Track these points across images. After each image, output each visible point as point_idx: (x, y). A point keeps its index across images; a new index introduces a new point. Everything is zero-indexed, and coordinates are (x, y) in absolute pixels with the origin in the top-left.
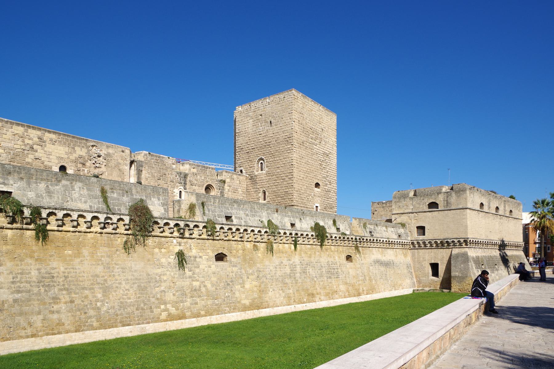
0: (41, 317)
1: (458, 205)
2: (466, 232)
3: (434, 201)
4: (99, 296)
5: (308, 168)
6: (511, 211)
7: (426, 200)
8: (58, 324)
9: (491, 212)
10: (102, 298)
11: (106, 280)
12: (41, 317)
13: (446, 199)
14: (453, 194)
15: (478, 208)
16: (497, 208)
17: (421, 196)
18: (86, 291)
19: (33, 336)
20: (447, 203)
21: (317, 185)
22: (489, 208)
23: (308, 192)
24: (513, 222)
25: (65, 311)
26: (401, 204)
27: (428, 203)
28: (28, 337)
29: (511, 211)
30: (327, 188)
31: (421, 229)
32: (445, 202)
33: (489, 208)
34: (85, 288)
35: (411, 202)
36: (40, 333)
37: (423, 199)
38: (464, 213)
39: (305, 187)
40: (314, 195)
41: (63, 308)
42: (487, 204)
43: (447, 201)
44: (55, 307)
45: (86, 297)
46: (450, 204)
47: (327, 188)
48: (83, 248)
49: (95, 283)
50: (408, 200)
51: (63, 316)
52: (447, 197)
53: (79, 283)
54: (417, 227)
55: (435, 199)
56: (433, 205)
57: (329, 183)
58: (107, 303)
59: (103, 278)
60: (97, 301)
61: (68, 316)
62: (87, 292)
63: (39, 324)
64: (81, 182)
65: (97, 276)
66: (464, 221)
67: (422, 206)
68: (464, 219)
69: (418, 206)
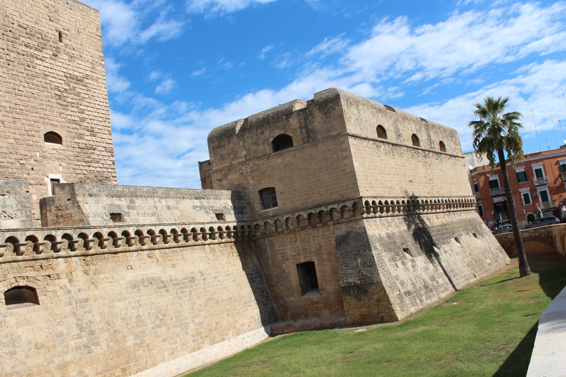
1: (328, 131)
2: (355, 187)
3: (282, 132)
5: (17, 102)
6: (442, 144)
7: (267, 133)
9: (404, 143)
13: (303, 125)
14: (317, 113)
15: (375, 136)
16: (415, 138)
17: (257, 128)
20: (308, 131)
21: (53, 137)
22: (399, 136)
23: (22, 152)
24: (448, 163)
26: (223, 152)
27: (271, 140)
29: (442, 144)
30: (83, 141)
31: (268, 196)
32: (304, 130)
33: (399, 136)
35: (241, 143)
37: (263, 133)
38: (344, 146)
39: (12, 141)
40: (44, 157)
42: (392, 128)
43: (306, 126)
46: (313, 131)
47: (83, 141)
50: (235, 139)
52: (306, 120)
54: (261, 192)
55: (284, 128)
56: (282, 143)
57: (88, 133)
66: (346, 162)
67: (261, 147)
68: (346, 158)
69: (253, 148)
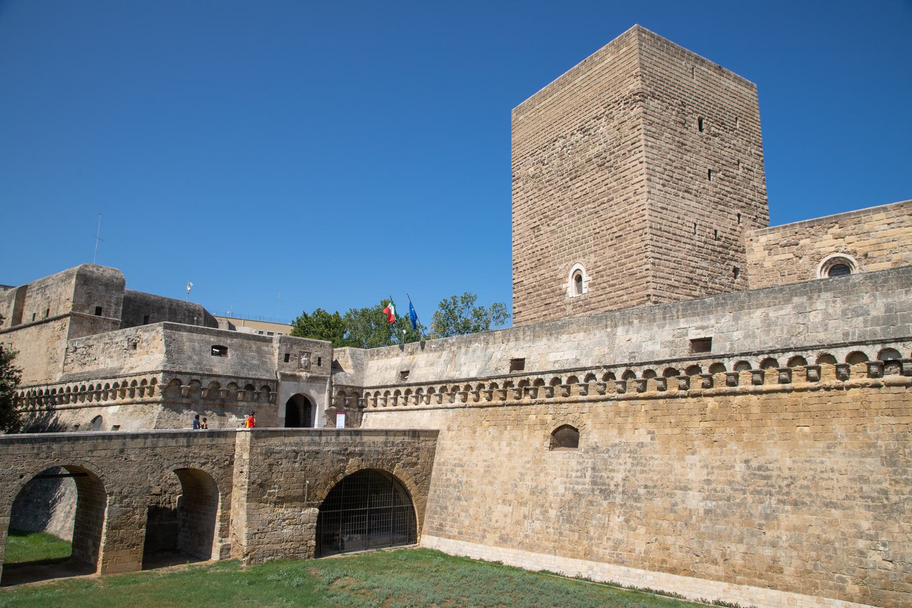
0: (742, 548)
4: (865, 525)
8: (770, 568)
10: (872, 532)
11: (885, 492)
12: (742, 548)
18: (833, 511)
19: (728, 579)
25: (786, 545)
28: (719, 579)
34: (831, 503)
36: (738, 578)
41: (784, 538)
44: (768, 533)
45: (833, 523)
48: (835, 420)
49: (857, 495)
51: (781, 553)
53: (820, 493)
58: (884, 545)
59: (879, 486)
60: (861, 535)
61: (791, 557)
62: (836, 513)
63: (738, 561)
64: (831, 290)
65: (865, 480)
